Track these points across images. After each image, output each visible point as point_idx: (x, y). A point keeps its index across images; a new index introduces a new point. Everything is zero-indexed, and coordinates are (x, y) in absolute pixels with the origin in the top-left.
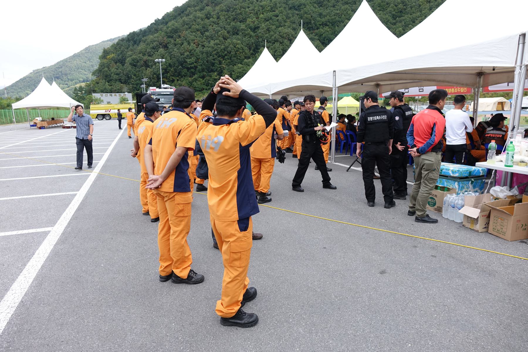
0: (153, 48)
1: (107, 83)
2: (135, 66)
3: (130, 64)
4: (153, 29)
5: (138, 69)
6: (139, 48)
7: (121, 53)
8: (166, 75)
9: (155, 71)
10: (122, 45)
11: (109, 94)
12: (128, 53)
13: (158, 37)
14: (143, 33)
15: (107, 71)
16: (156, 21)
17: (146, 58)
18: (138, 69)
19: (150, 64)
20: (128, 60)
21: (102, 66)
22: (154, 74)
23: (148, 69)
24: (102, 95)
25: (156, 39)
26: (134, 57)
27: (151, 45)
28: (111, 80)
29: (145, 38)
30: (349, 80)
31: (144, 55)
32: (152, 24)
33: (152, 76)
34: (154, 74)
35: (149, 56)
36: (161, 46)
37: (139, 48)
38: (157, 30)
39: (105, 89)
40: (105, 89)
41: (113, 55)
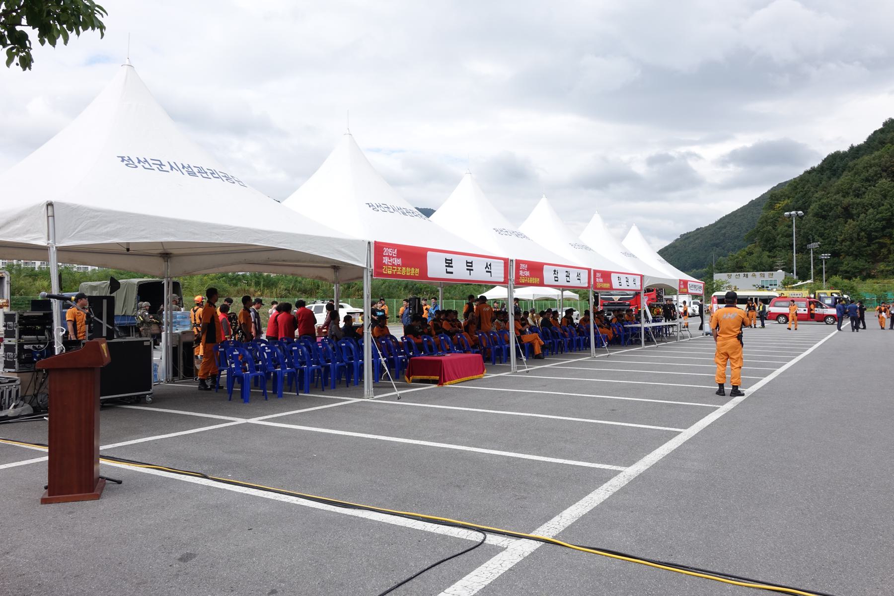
0: (867, 180)
1: (767, 253)
2: (824, 217)
3: (816, 215)
4: (876, 143)
5: (829, 224)
6: (839, 182)
7: (803, 196)
8: (888, 230)
9: (864, 223)
10: (808, 181)
11: (742, 274)
12: (816, 195)
13: (880, 157)
14: (855, 152)
15: (769, 232)
16: (885, 124)
17: (847, 201)
18: (829, 224)
19: (854, 212)
20: (814, 207)
21: (762, 223)
22: (862, 230)
23: (850, 221)
24: (730, 277)
25: (877, 161)
26: (825, 201)
27: (865, 175)
28: (775, 247)
29: (855, 161)
30: (349, 257)
31: (846, 194)
32: (875, 132)
33: (855, 235)
34: (862, 230)
35: (858, 196)
36: (885, 174)
37: (839, 182)
38: (882, 143)
39: (761, 263)
40: (761, 263)
41: (786, 202)
